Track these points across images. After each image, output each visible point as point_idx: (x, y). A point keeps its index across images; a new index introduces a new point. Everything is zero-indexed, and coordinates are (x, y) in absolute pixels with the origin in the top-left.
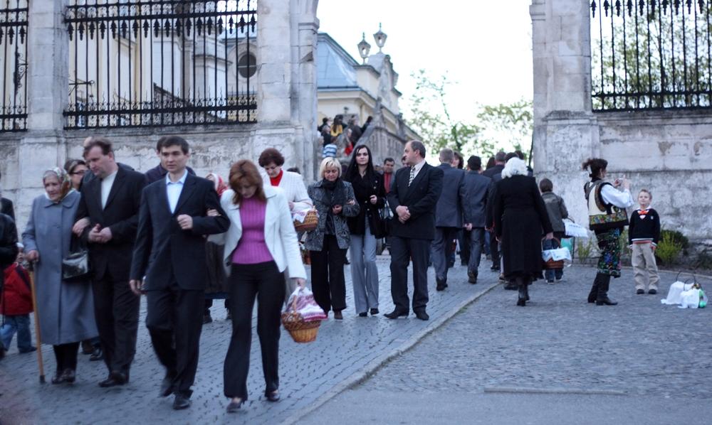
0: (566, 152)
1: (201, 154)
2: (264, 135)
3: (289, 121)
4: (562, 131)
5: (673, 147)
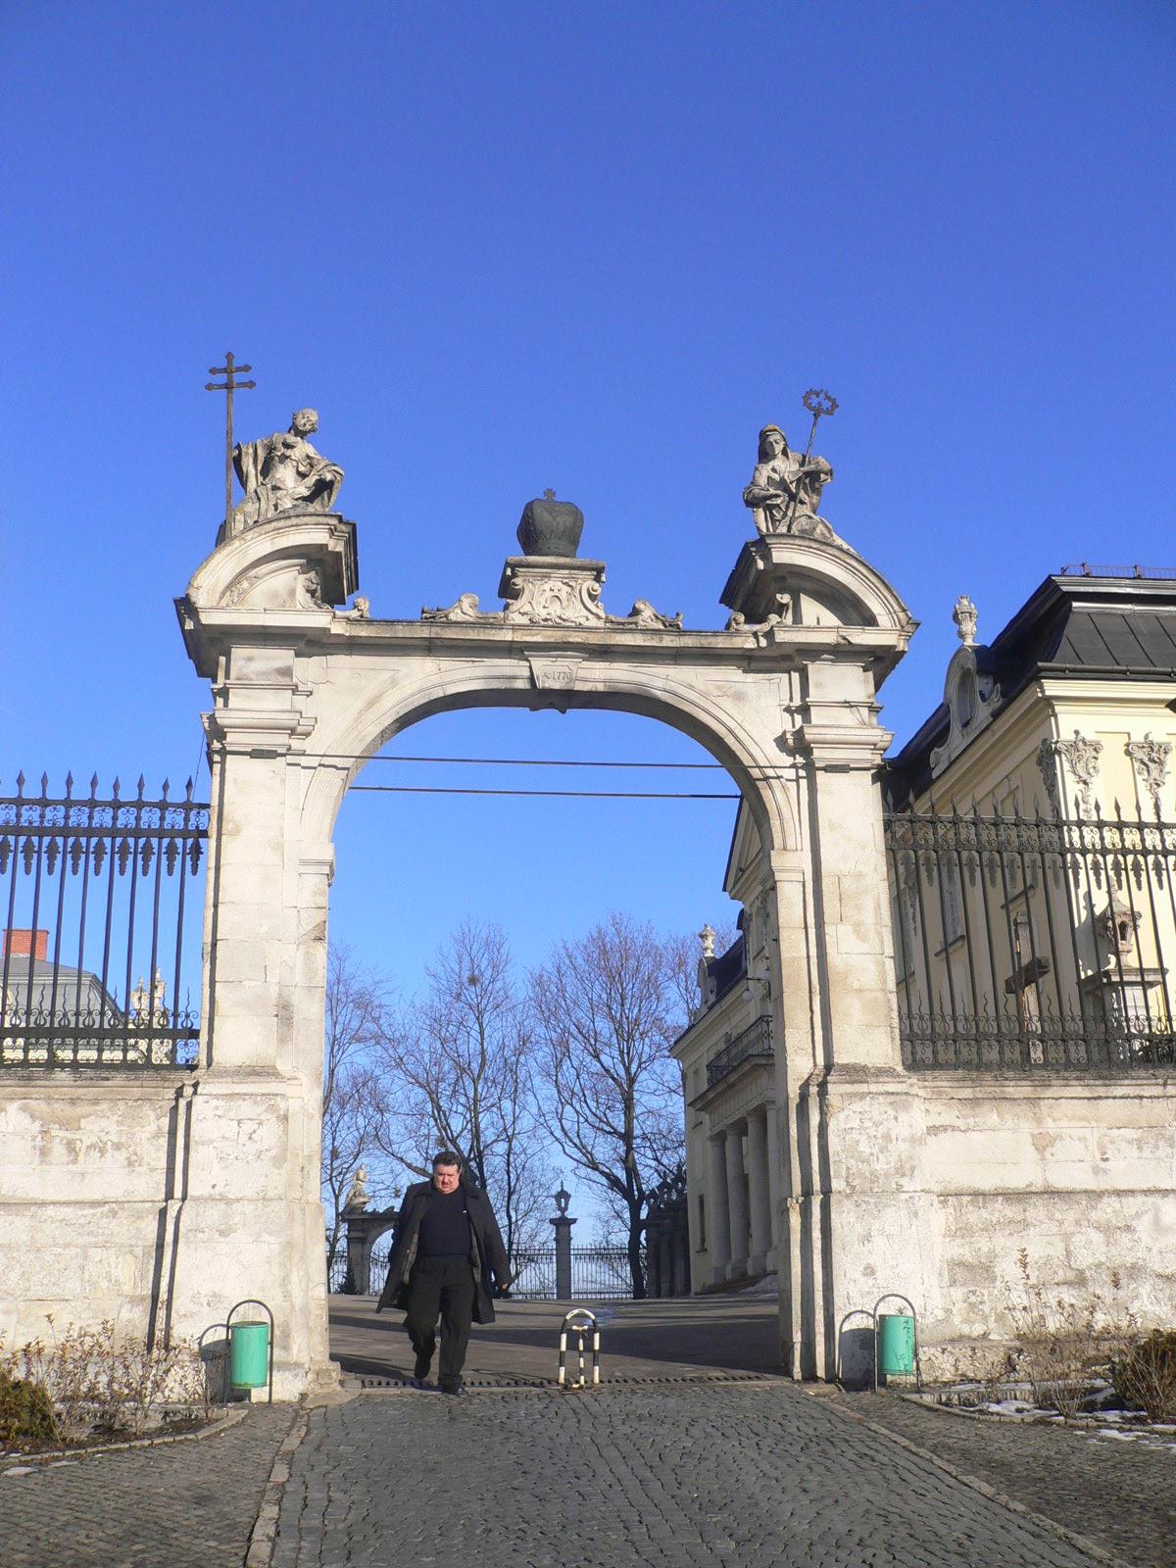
0: (868, 1151)
1: (62, 1134)
2: (217, 1096)
3: (274, 1067)
4: (858, 1106)
5: (1058, 1144)
